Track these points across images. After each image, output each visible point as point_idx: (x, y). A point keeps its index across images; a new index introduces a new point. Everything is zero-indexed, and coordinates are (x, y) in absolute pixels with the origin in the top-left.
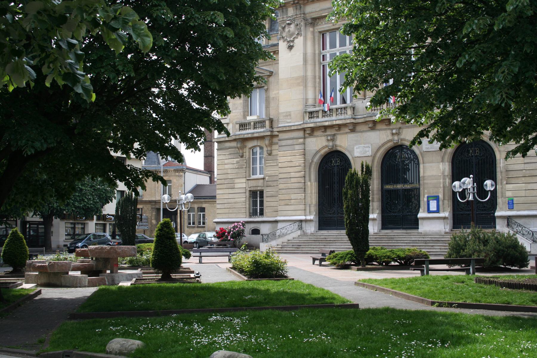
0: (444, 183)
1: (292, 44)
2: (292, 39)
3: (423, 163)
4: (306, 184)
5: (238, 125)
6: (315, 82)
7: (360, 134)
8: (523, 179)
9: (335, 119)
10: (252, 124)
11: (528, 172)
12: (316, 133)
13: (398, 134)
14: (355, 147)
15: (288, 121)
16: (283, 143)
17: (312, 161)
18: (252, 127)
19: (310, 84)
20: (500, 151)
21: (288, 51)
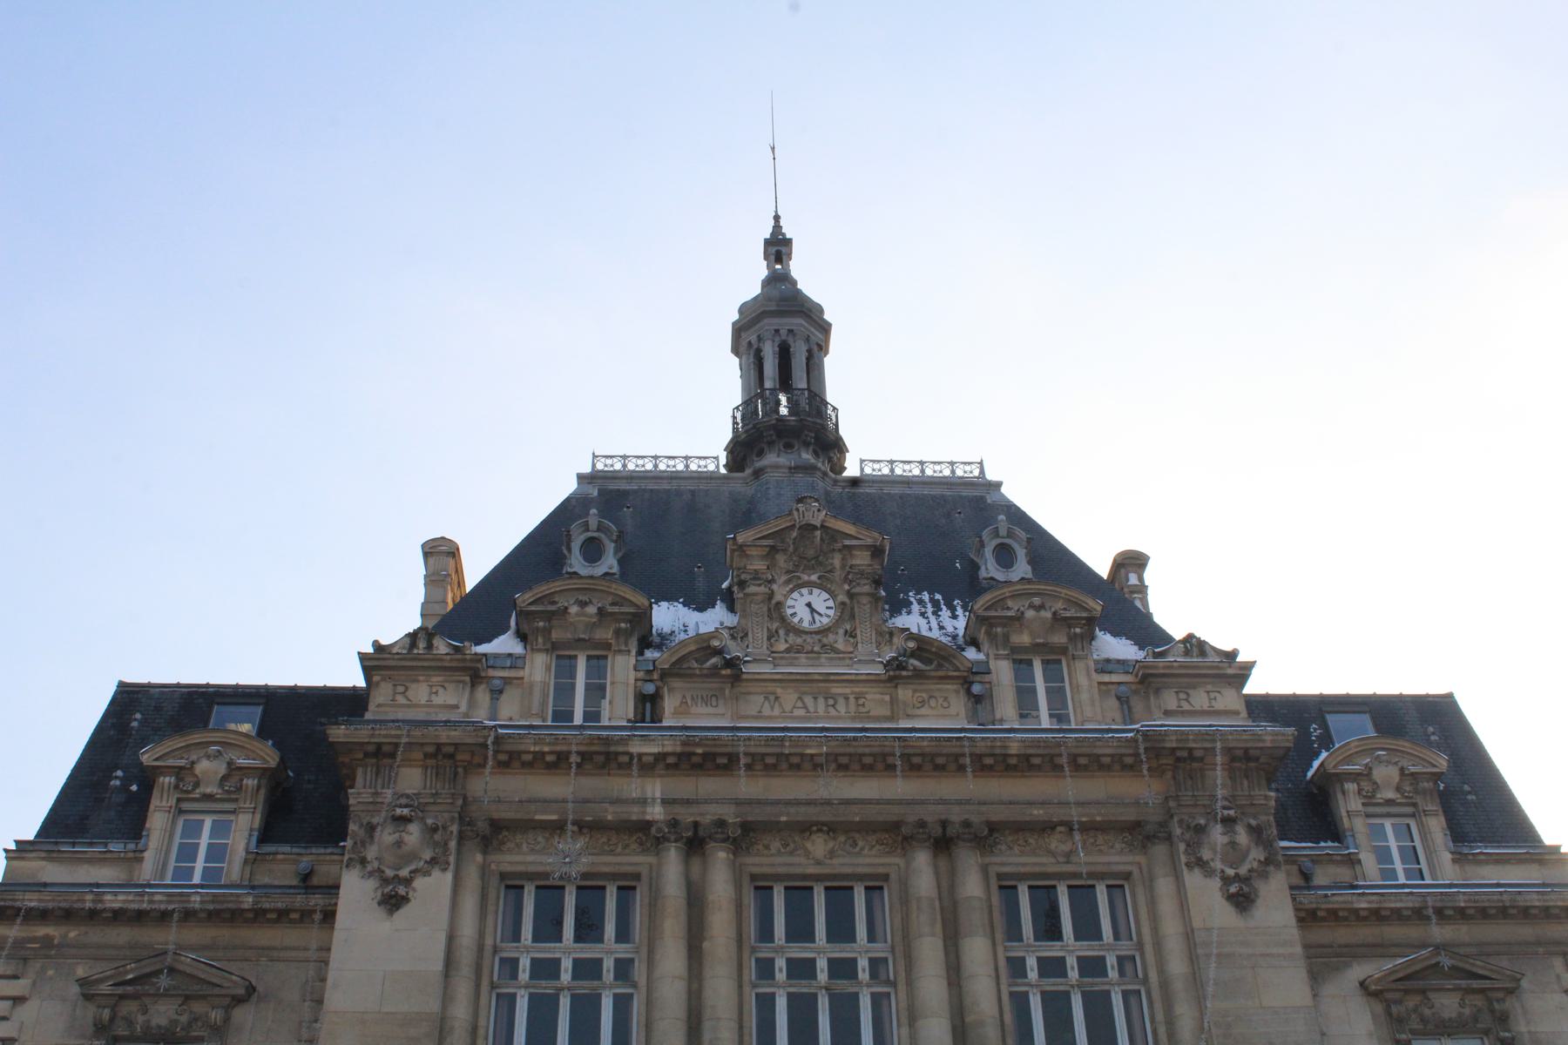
1: (402, 890)
2: (404, 873)
21: (380, 913)
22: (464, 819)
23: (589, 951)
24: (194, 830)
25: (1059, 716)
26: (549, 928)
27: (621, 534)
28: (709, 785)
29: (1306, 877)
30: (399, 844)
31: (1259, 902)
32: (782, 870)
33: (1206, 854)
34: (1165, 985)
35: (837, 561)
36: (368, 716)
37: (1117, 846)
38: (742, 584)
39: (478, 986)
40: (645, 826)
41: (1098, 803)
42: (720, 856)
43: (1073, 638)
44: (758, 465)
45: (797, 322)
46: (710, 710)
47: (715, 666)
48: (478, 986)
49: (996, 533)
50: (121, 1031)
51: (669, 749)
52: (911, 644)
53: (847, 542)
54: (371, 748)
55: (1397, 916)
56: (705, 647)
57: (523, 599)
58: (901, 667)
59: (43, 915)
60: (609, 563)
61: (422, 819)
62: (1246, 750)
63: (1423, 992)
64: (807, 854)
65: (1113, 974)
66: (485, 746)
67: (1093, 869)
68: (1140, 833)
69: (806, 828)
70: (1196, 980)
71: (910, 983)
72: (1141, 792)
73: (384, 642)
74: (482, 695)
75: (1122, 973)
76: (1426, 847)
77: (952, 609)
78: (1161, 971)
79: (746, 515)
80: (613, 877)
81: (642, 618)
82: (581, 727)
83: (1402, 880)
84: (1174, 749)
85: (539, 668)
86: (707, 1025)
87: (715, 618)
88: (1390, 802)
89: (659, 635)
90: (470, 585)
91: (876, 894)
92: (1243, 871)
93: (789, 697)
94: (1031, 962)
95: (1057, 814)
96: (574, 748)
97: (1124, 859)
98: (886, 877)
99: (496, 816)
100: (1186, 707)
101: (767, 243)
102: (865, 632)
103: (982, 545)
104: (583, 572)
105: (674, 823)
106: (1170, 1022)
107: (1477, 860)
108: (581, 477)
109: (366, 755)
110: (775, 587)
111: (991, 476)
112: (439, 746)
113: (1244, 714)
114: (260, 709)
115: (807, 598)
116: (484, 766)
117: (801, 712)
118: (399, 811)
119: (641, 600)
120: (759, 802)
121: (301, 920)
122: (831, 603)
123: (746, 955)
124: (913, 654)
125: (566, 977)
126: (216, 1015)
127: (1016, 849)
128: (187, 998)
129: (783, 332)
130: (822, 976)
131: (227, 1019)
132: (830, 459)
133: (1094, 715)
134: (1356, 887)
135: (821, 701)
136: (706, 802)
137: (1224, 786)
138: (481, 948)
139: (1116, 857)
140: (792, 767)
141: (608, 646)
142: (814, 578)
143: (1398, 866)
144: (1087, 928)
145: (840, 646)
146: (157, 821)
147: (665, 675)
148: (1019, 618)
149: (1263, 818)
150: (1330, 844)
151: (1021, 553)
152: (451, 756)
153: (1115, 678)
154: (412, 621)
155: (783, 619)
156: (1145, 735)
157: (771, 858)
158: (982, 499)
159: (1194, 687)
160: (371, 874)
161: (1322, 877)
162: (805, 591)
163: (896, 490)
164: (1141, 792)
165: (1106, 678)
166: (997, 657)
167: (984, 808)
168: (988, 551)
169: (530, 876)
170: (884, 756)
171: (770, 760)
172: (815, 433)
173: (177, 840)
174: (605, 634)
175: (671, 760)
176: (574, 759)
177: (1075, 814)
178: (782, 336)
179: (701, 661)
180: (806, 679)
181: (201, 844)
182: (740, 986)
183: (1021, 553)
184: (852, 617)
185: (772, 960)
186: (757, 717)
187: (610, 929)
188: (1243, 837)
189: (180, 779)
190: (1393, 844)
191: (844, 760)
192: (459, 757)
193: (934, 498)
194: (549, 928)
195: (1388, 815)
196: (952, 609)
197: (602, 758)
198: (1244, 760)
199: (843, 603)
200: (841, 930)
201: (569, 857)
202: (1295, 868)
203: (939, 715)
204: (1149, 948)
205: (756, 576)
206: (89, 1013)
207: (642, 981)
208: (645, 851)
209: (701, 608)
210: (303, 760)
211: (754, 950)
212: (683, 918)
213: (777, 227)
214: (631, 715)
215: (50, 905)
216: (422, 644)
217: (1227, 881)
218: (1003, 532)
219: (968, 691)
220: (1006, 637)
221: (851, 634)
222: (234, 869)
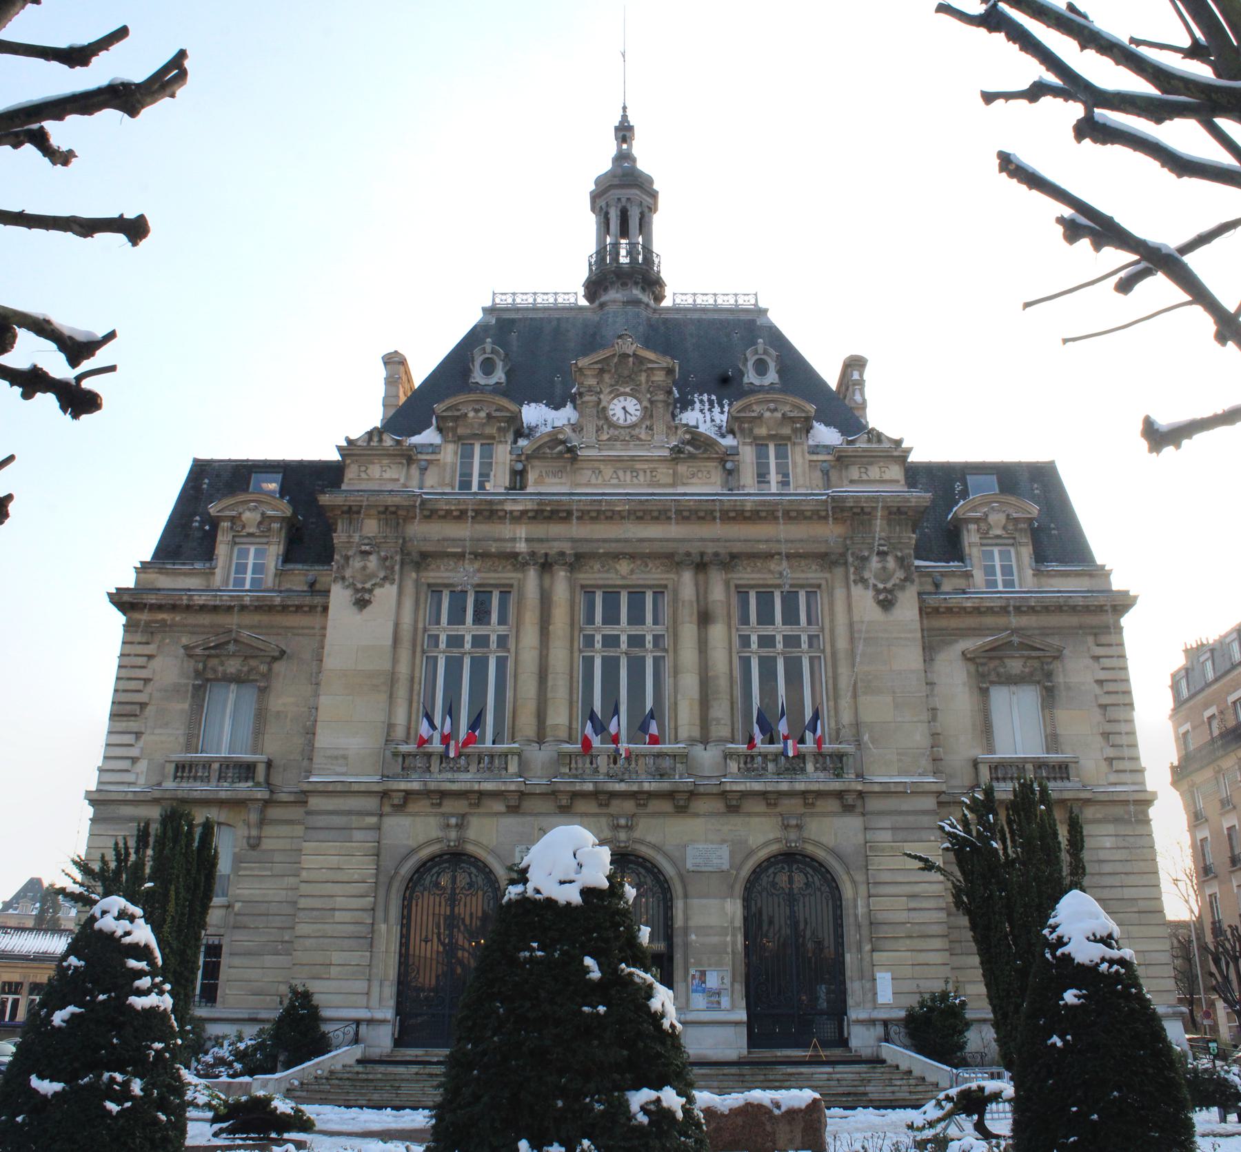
0: (734, 943)
1: (367, 596)
2: (368, 586)
3: (686, 896)
4: (376, 927)
5: (173, 765)
6: (411, 690)
7: (529, 818)
8: (908, 942)
9: (466, 780)
10: (216, 766)
11: (917, 927)
12: (412, 807)
13: (629, 828)
14: (517, 849)
15: (339, 769)
16: (321, 821)
17: (396, 873)
18: (214, 776)
19: (402, 692)
20: (854, 882)
21: (355, 609)
22: (403, 551)
23: (481, 630)
24: (244, 554)
25: (785, 483)
26: (457, 617)
27: (507, 355)
28: (556, 529)
29: (937, 585)
30: (364, 568)
31: (898, 605)
32: (600, 582)
33: (866, 575)
34: (834, 654)
35: (643, 378)
36: (344, 487)
37: (813, 567)
38: (581, 394)
39: (414, 652)
40: (515, 555)
41: (801, 541)
42: (561, 574)
43: (795, 430)
44: (603, 299)
45: (635, 192)
46: (557, 480)
47: (560, 451)
48: (414, 652)
49: (756, 352)
50: (211, 676)
51: (529, 507)
52: (688, 436)
53: (650, 366)
54: (345, 508)
55: (990, 611)
56: (555, 439)
57: (439, 407)
58: (680, 451)
59: (160, 608)
60: (499, 376)
61: (378, 552)
62: (899, 508)
63: (1001, 658)
64: (617, 571)
65: (805, 646)
66: (414, 506)
67: (795, 582)
68: (827, 560)
69: (616, 556)
70: (852, 653)
71: (675, 651)
72: (830, 533)
73: (352, 437)
74: (414, 471)
75: (810, 645)
76: (1019, 566)
77: (722, 406)
78: (833, 646)
79: (592, 339)
80: (496, 586)
81: (515, 419)
82: (475, 494)
83: (1000, 588)
84: (851, 508)
85: (449, 454)
86: (550, 677)
87: (564, 416)
88: (998, 537)
89: (528, 427)
90: (417, 383)
91: (659, 596)
92: (889, 585)
93: (608, 471)
94: (754, 638)
95: (774, 547)
96: (470, 507)
97: (818, 575)
98: (666, 586)
99: (424, 549)
100: (865, 477)
101: (617, 129)
102: (660, 427)
103: (746, 360)
104: (482, 382)
105: (533, 554)
106: (835, 678)
107: (1050, 575)
108: (485, 310)
109: (343, 512)
110: (602, 396)
111: (762, 305)
112: (387, 507)
113: (903, 482)
114: (280, 476)
115: (623, 404)
116: (415, 518)
117: (615, 481)
118: (363, 548)
119: (513, 407)
120: (586, 540)
121: (310, 611)
122: (638, 407)
123: (576, 634)
124: (689, 443)
125: (468, 646)
126: (263, 668)
127: (749, 569)
128: (246, 658)
129: (624, 200)
130: (624, 646)
131: (270, 670)
132: (653, 293)
133: (805, 484)
134: (965, 593)
135: (628, 473)
136: (555, 540)
137: (882, 530)
138: (415, 629)
139: (813, 574)
140: (607, 518)
141: (494, 438)
142: (628, 390)
143: (999, 578)
144: (791, 617)
145: (643, 436)
146: (221, 550)
147: (529, 457)
148: (760, 417)
149: (907, 551)
150: (956, 564)
151: (772, 366)
152: (394, 513)
153: (820, 457)
154: (375, 418)
155: (606, 419)
156: (833, 498)
157: (593, 575)
158: (753, 322)
159: (871, 464)
160: (347, 587)
161: (947, 586)
162: (622, 398)
163: (696, 316)
164: (830, 533)
165: (815, 458)
166: (744, 444)
167: (727, 544)
168: (750, 364)
169: (446, 586)
170: (666, 511)
171: (594, 514)
172: (645, 277)
173: (235, 561)
174: (489, 430)
175: (530, 514)
176: (470, 514)
177: (784, 549)
178: (624, 199)
179: (552, 448)
180: (619, 459)
181: (249, 563)
182: (572, 652)
183: (772, 366)
184: (651, 416)
185: (593, 636)
186: (588, 485)
187: (494, 617)
188: (891, 563)
189: (233, 523)
190: (997, 563)
191: (640, 514)
192: (400, 512)
193: (721, 321)
194: (457, 617)
195: (997, 545)
196: (722, 406)
197: (487, 514)
198: (897, 514)
199: (646, 407)
200: (636, 617)
201: (466, 575)
202: (930, 580)
203: (704, 485)
204: (827, 631)
205: (590, 389)
206: (190, 665)
207: (513, 649)
208: (516, 570)
209: (556, 408)
210: (307, 507)
211: (581, 630)
212: (537, 613)
213: (625, 117)
214: (507, 484)
215: (163, 602)
216: (376, 439)
217: (878, 592)
218: (760, 351)
219: (724, 467)
220: (751, 430)
221: (650, 428)
222: (269, 579)
